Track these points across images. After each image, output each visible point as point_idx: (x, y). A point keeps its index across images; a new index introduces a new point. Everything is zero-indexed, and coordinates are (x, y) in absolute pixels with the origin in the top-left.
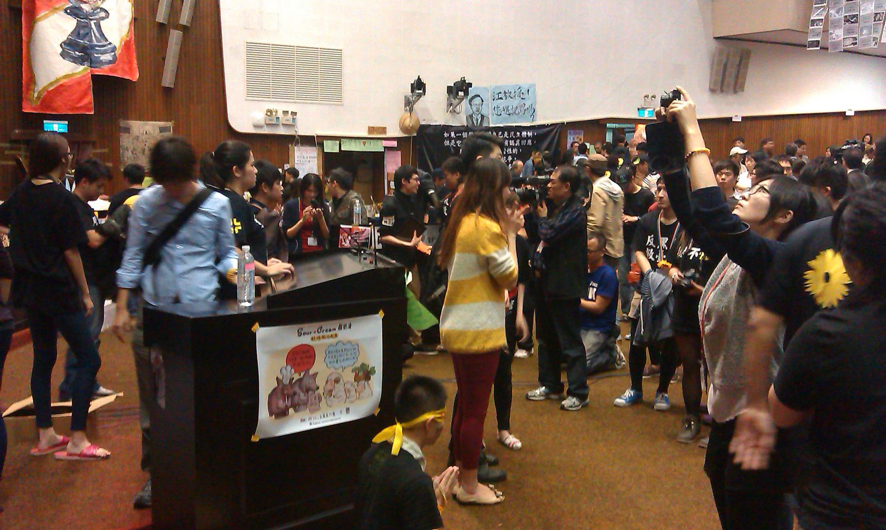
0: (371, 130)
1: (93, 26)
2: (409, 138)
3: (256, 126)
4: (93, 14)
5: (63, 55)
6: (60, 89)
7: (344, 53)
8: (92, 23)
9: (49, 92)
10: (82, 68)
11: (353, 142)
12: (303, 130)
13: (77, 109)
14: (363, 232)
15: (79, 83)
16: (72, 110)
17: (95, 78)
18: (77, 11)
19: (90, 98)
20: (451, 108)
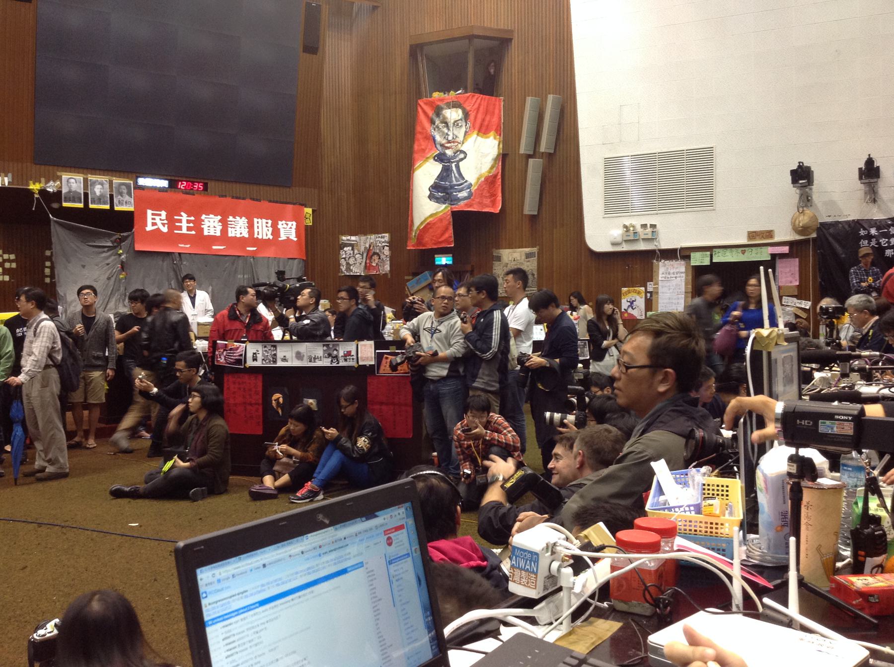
0: (752, 235)
1: (454, 168)
2: (806, 242)
3: (613, 244)
4: (454, 157)
5: (431, 197)
6: (428, 227)
7: (717, 152)
8: (453, 165)
9: (421, 231)
10: (444, 206)
11: (728, 252)
12: (666, 243)
13: (441, 242)
14: (237, 348)
15: (441, 220)
16: (435, 244)
17: (455, 214)
18: (443, 157)
19: (450, 232)
20: (873, 196)
